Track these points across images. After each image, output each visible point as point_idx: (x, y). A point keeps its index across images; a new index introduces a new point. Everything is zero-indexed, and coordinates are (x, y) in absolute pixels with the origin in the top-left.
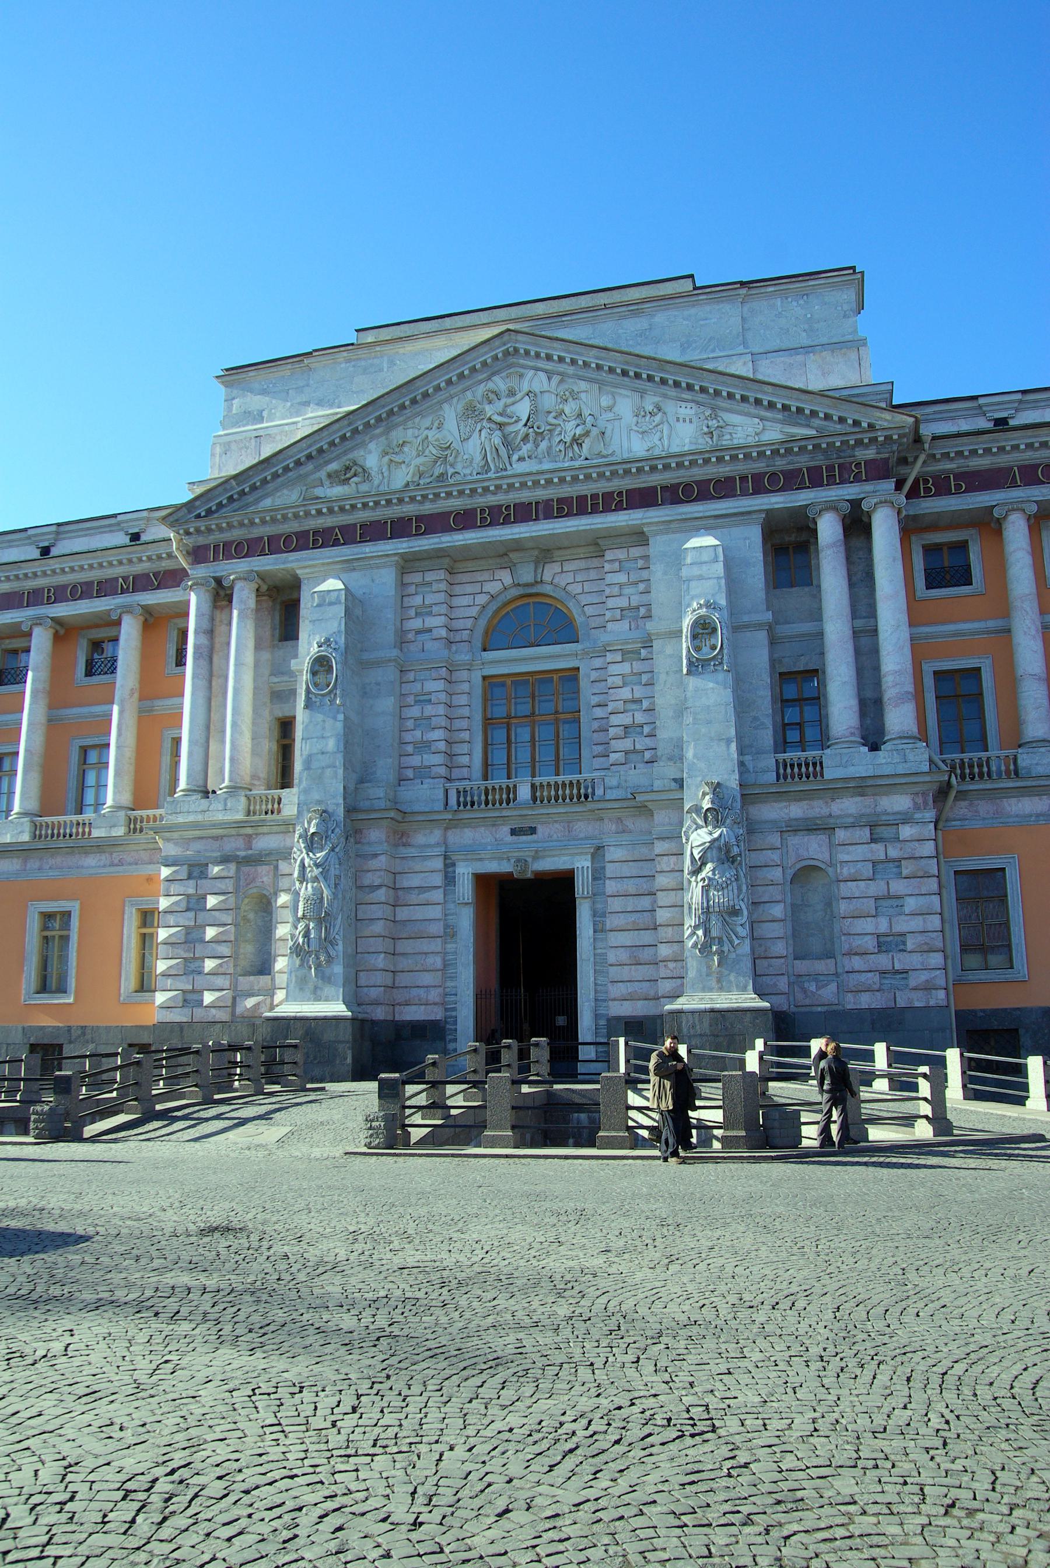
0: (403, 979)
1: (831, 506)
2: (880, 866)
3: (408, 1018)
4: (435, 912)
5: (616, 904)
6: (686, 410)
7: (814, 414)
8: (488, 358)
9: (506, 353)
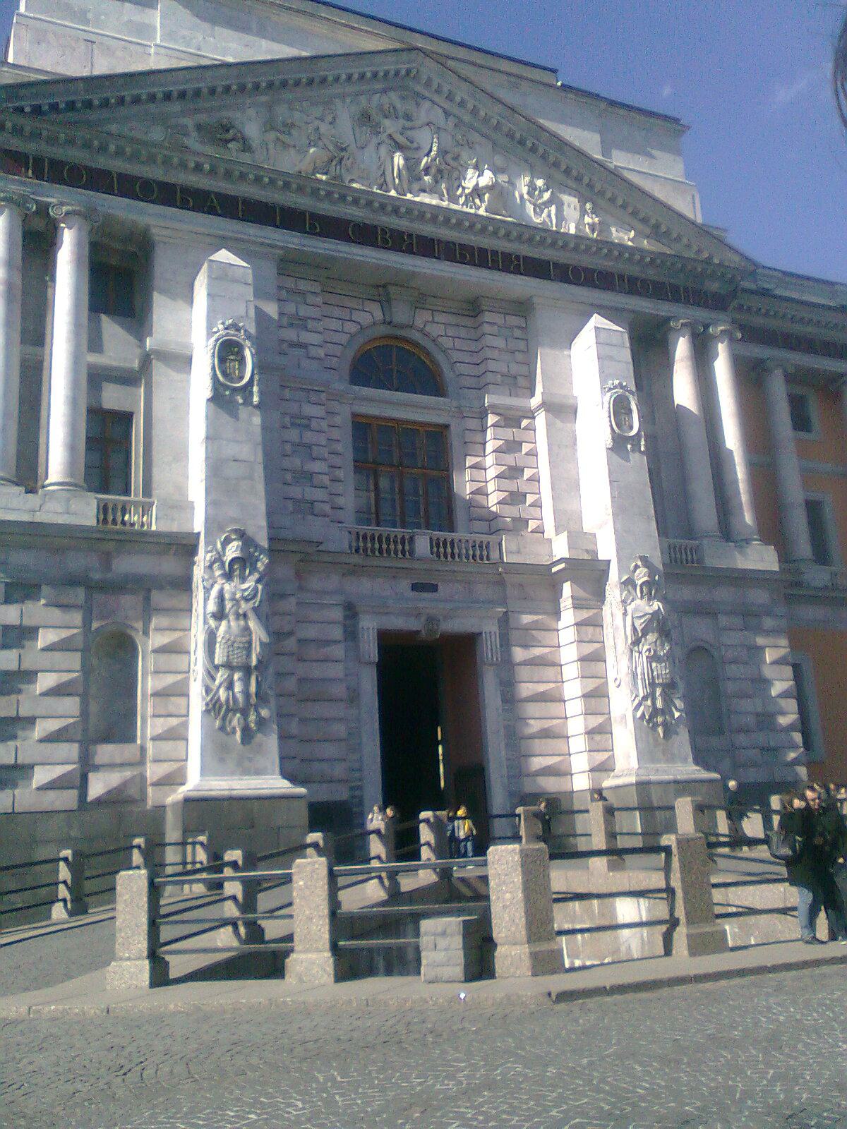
4: (336, 671)
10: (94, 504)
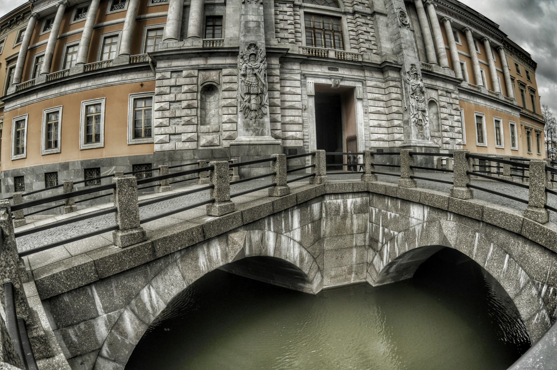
10: (202, 41)
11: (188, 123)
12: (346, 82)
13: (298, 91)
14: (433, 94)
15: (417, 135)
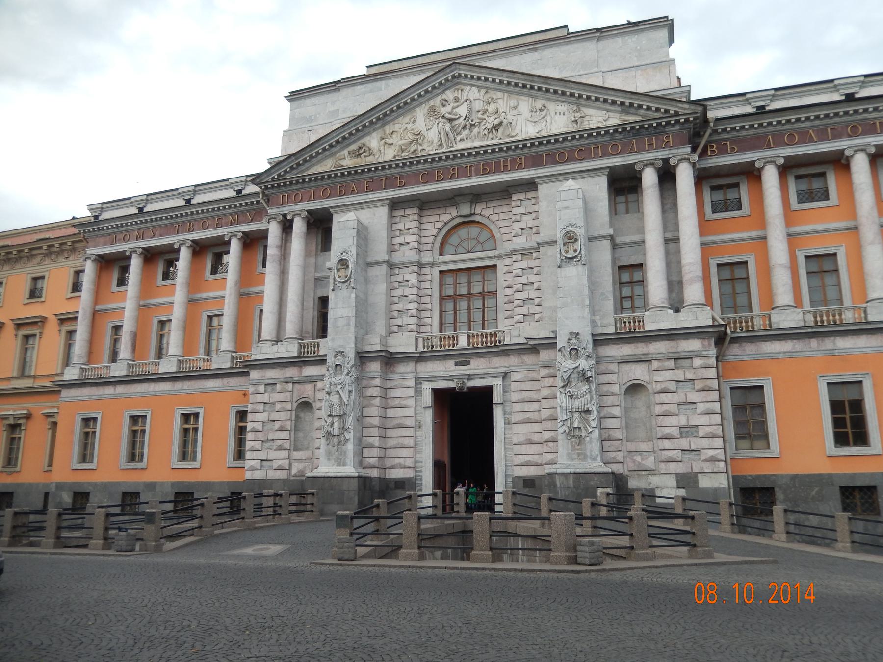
0: (391, 453)
1: (650, 164)
2: (681, 384)
3: (394, 476)
4: (410, 412)
5: (518, 407)
6: (562, 108)
7: (640, 107)
8: (443, 80)
9: (454, 77)
10: (297, 345)
11: (280, 448)
12: (477, 380)
13: (411, 402)
14: (638, 373)
15: (568, 454)
